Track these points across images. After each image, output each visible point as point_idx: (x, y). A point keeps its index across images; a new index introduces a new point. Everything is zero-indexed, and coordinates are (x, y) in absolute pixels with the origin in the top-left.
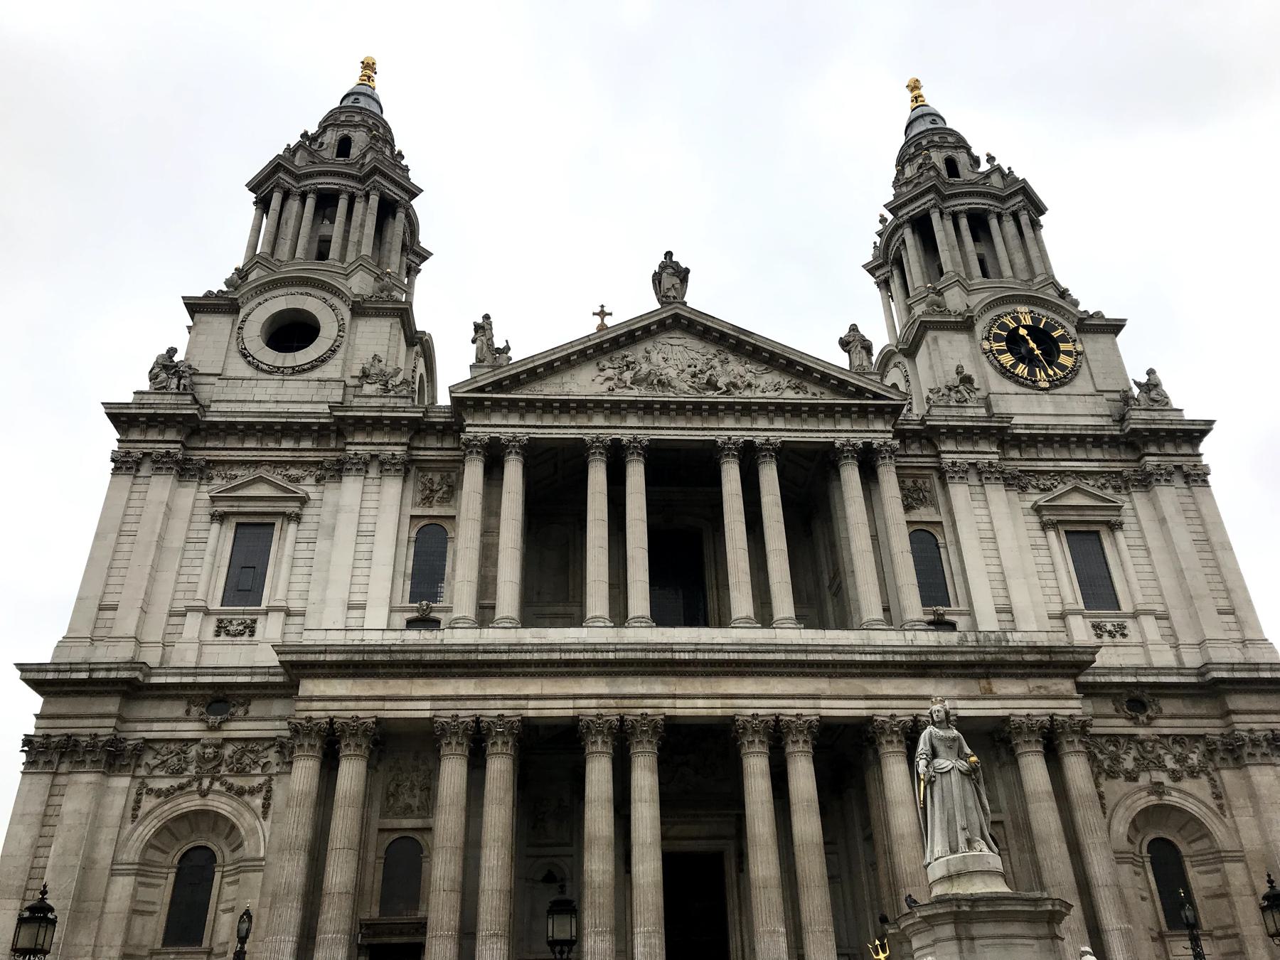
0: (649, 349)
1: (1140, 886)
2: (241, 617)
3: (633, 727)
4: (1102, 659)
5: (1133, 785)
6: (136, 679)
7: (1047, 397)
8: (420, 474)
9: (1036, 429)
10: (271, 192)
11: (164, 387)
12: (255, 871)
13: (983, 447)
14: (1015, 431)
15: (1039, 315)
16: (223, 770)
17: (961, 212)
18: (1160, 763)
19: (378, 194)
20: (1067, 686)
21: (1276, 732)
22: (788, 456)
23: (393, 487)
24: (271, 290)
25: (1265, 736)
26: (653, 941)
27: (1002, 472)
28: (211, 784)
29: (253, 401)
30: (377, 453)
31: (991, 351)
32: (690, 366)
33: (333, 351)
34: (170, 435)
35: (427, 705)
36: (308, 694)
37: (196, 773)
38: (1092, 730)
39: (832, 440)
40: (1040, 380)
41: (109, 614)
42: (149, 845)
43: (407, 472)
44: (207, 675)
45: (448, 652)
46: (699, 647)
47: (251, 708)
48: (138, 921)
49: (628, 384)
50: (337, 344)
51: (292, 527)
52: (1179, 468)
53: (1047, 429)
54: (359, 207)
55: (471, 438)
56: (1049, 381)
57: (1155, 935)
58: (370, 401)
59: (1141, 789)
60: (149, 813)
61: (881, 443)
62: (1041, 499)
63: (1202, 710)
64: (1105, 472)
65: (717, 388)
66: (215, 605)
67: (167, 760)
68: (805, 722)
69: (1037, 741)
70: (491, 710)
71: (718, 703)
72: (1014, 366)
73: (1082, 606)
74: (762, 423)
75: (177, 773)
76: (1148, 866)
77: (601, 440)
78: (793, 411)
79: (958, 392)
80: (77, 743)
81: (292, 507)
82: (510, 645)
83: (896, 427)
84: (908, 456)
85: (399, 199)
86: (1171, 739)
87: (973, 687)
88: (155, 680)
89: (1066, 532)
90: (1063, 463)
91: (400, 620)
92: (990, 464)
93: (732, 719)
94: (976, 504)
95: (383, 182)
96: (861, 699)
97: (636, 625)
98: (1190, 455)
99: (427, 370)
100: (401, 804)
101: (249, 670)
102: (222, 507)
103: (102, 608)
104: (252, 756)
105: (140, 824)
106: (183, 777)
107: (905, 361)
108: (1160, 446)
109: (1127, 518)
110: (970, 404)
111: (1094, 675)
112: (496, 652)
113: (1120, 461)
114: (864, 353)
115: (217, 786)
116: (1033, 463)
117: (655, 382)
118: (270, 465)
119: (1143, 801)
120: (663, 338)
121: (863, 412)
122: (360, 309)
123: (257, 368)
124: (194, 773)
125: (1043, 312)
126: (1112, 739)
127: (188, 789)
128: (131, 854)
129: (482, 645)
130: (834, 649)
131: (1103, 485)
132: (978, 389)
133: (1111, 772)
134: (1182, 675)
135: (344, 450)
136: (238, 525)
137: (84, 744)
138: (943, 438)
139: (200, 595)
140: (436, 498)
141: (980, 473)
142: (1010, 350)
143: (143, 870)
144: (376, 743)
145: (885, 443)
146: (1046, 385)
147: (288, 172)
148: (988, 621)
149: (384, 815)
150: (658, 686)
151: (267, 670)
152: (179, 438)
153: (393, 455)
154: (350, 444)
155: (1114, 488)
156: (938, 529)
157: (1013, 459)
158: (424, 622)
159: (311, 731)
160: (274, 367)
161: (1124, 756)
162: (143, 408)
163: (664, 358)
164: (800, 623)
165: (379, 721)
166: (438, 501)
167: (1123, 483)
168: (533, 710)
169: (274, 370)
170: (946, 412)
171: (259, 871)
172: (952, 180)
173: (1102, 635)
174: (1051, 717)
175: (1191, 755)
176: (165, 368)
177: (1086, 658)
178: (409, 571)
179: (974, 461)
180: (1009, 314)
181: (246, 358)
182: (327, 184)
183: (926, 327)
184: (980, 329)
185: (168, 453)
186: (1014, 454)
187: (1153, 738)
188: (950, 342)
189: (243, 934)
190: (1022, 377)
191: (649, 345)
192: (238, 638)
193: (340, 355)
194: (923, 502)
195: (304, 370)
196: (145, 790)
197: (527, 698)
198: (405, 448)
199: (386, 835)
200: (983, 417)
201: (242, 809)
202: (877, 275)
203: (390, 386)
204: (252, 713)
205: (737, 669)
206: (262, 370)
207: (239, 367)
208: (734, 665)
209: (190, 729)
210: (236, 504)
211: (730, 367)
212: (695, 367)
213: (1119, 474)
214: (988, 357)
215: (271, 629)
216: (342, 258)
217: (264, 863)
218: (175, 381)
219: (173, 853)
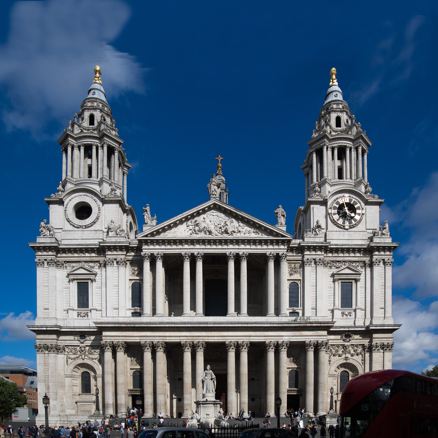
9: (339, 246)
13: (319, 253)
14: (332, 247)
19: (107, 146)
22: (251, 258)
24: (73, 194)
29: (74, 239)
30: (116, 258)
33: (97, 218)
35: (138, 338)
40: (346, 226)
53: (343, 246)
54: (100, 151)
56: (349, 226)
58: (112, 240)
62: (335, 271)
64: (359, 261)
68: (245, 343)
72: (338, 220)
73: (340, 307)
79: (315, 231)
81: (92, 277)
87: (297, 333)
89: (341, 282)
92: (320, 259)
94: (312, 273)
97: (198, 316)
102: (71, 277)
108: (379, 251)
109: (362, 277)
110: (319, 236)
116: (336, 258)
122: (104, 201)
123: (73, 226)
130: (255, 323)
135: (105, 257)
141: (315, 263)
142: (339, 213)
147: (72, 137)
150: (204, 334)
153: (121, 259)
154: (107, 255)
156: (300, 281)
158: (135, 314)
163: (210, 221)
165: (125, 342)
168: (168, 340)
174: (317, 341)
180: (341, 197)
181: (69, 222)
183: (310, 203)
184: (329, 203)
186: (330, 255)
190: (340, 224)
193: (100, 220)
195: (89, 226)
197: (166, 336)
198: (125, 256)
203: (118, 233)
207: (68, 227)
213: (364, 261)
214: (330, 216)
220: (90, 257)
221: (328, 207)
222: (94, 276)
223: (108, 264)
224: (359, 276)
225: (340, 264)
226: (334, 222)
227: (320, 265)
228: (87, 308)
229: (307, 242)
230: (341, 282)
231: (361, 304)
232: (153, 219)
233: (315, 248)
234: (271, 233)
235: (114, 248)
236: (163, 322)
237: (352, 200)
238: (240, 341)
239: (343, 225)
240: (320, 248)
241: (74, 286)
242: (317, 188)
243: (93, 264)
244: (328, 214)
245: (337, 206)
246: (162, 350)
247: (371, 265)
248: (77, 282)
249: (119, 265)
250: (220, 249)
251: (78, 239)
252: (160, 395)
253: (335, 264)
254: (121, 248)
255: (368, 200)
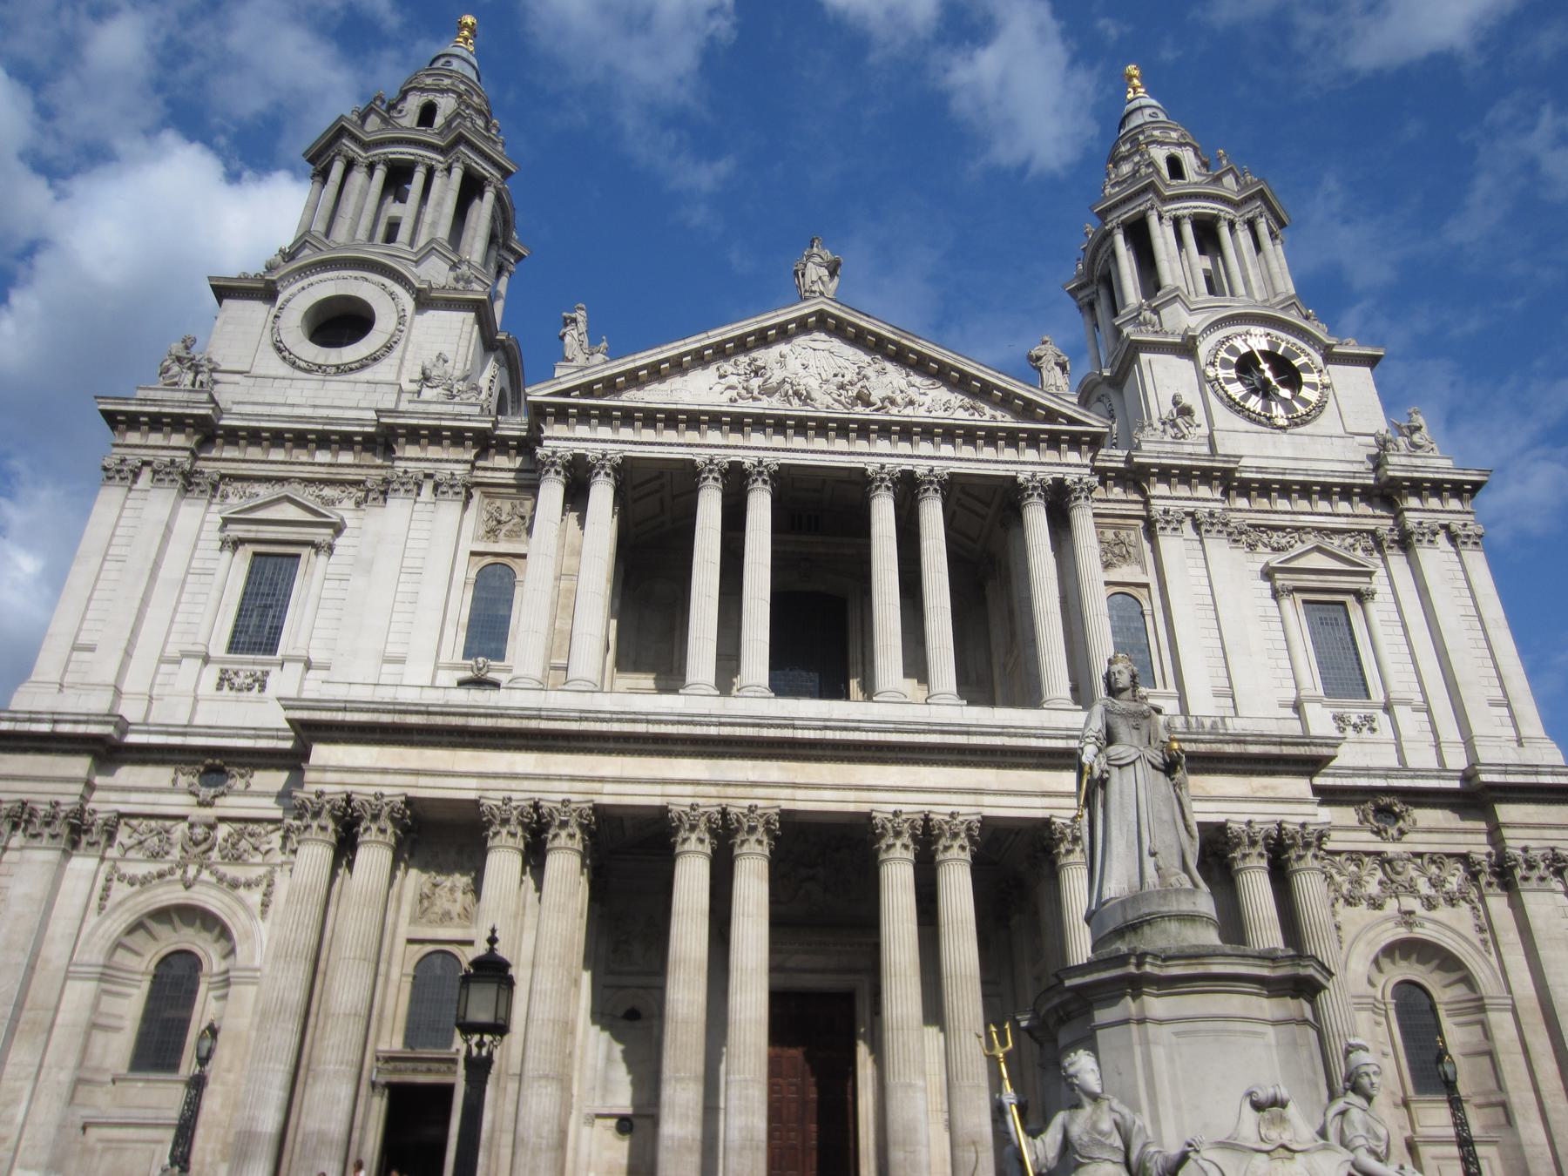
0: (784, 352)
1: (1381, 1040)
2: (250, 667)
3: (738, 821)
4: (1346, 756)
5: (1377, 913)
6: (108, 736)
7: (1284, 437)
8: (487, 501)
9: (1270, 473)
10: (331, 164)
11: (176, 384)
12: (247, 983)
13: (1203, 491)
14: (1245, 475)
15: (1277, 338)
16: (215, 855)
17: (1184, 217)
18: (1411, 887)
20: (1299, 786)
21: (1557, 851)
22: (957, 490)
23: (449, 510)
25: (1543, 855)
26: (750, 1091)
27: (1226, 525)
28: (199, 872)
29: (284, 405)
30: (432, 472)
31: (1217, 379)
32: (835, 375)
33: (389, 348)
34: (178, 439)
35: (473, 783)
36: (321, 762)
37: (181, 857)
38: (1329, 846)
39: (1014, 474)
40: (1276, 417)
41: (86, 656)
42: (118, 945)
43: (469, 496)
44: (200, 735)
45: (502, 716)
46: (828, 724)
47: (251, 781)
48: (99, 1038)
49: (756, 393)
50: (394, 339)
51: (322, 558)
52: (1446, 527)
53: (1284, 474)
54: (437, 182)
55: (550, 454)
56: (1288, 418)
57: (1399, 1101)
59: (1387, 919)
60: (120, 903)
61: (1076, 480)
63: (1469, 824)
64: (1354, 530)
65: (868, 404)
66: (219, 648)
67: (146, 840)
68: (962, 823)
69: (1261, 855)
70: (552, 796)
71: (851, 795)
72: (1245, 398)
73: (1321, 692)
74: (925, 448)
75: (155, 856)
76: (1392, 1015)
77: (715, 462)
78: (970, 435)
79: (1174, 425)
80: (33, 813)
81: (322, 535)
82: (582, 711)
83: (1097, 464)
84: (1108, 501)
85: (488, 175)
86: (1426, 858)
88: (132, 739)
89: (1305, 602)
90: (1302, 518)
91: (448, 678)
92: (1211, 515)
93: (868, 816)
94: (1190, 562)
95: (471, 155)
96: (1036, 796)
98: (1459, 512)
99: (511, 381)
100: (436, 909)
101: (253, 732)
102: (237, 531)
103: (76, 648)
104: (252, 840)
105: (108, 916)
106: (166, 862)
107: (1112, 394)
111: (1334, 775)
112: (563, 720)
113: (1374, 517)
114: (1058, 369)
115: (205, 875)
117: (790, 392)
118: (300, 484)
119: (1390, 933)
120: (802, 340)
121: (1054, 441)
122: (425, 300)
123: (293, 364)
124: (178, 858)
125: (1283, 335)
126: (1354, 857)
127: (169, 878)
128: (93, 954)
129: (547, 710)
130: (1003, 731)
131: (1352, 545)
132: (1199, 426)
133: (1351, 897)
134: (1443, 778)
136: (255, 554)
137: (42, 813)
138: (1153, 479)
139: (201, 639)
140: (503, 531)
141: (1197, 526)
142: (1239, 379)
143: (107, 975)
144: (406, 830)
145: (1080, 480)
146: (1282, 422)
148: (1204, 705)
149: (414, 920)
151: (274, 733)
152: (188, 445)
153: (452, 474)
154: (400, 459)
155: (1365, 550)
156: (1144, 591)
157: (1240, 510)
159: (321, 809)
160: (315, 364)
161: (1368, 878)
162: (145, 405)
164: (962, 698)
165: (410, 802)
166: (506, 535)
167: (1377, 543)
168: (610, 796)
169: (311, 369)
170: (1159, 448)
171: (253, 984)
172: (1174, 182)
173: (1344, 729)
174: (1280, 825)
175: (1450, 879)
176: (179, 360)
177: (1325, 751)
178: (465, 619)
179: (1192, 510)
180: (1240, 336)
182: (401, 153)
184: (1204, 349)
185: (172, 462)
186: (1242, 503)
187: (1405, 856)
188: (1166, 368)
189: (204, 1053)
190: (1254, 412)
191: (783, 348)
192: (245, 693)
193: (397, 351)
194: (1124, 558)
195: (351, 370)
196: (116, 876)
197: (602, 780)
198: (468, 466)
199: (416, 947)
200: (1205, 455)
201: (235, 906)
202: (1080, 296)
203: (455, 392)
204: (253, 787)
205: (879, 754)
206: (299, 368)
208: (873, 748)
209: (178, 803)
210: (254, 528)
211: (885, 379)
212: (843, 376)
213: (1373, 533)
214: (1213, 386)
215: (284, 682)
216: (412, 243)
217: (258, 974)
218: (191, 376)
219: (148, 957)
220: (331, 465)
221: (1202, 362)
222: (330, 531)
223: (396, 490)
224: (1367, 580)
225: (1284, 537)
226: (1232, 403)
227: (1214, 534)
228: (270, 654)
229: (1159, 452)
230: (1305, 602)
231: (1402, 683)
232: (594, 350)
233: (1186, 475)
234: (1028, 409)
235: (435, 436)
236: (599, 712)
237: (1280, 345)
238: (940, 814)
239: (1265, 416)
240: (1206, 476)
241: (237, 569)
242: (1148, 314)
243: (338, 491)
244: (1203, 379)
245: (1234, 360)
246: (577, 844)
247: (1405, 542)
248: (255, 554)
249: (441, 497)
250: (842, 453)
251: (298, 406)
252: (543, 1082)
253: (1265, 535)
254: (458, 437)
255: (1333, 345)
